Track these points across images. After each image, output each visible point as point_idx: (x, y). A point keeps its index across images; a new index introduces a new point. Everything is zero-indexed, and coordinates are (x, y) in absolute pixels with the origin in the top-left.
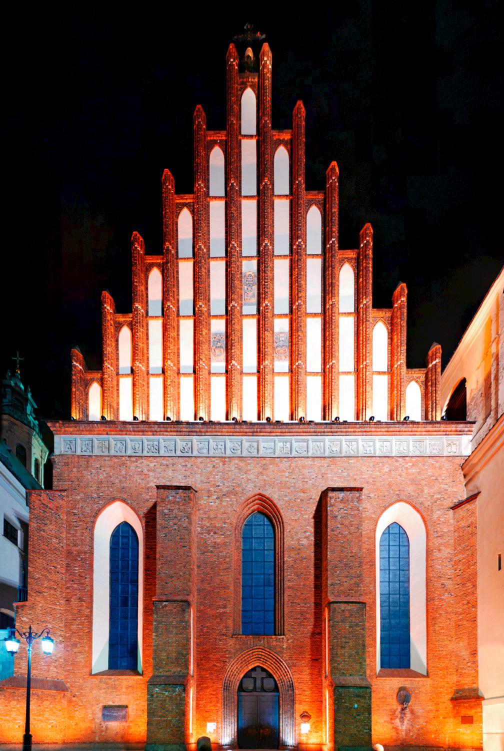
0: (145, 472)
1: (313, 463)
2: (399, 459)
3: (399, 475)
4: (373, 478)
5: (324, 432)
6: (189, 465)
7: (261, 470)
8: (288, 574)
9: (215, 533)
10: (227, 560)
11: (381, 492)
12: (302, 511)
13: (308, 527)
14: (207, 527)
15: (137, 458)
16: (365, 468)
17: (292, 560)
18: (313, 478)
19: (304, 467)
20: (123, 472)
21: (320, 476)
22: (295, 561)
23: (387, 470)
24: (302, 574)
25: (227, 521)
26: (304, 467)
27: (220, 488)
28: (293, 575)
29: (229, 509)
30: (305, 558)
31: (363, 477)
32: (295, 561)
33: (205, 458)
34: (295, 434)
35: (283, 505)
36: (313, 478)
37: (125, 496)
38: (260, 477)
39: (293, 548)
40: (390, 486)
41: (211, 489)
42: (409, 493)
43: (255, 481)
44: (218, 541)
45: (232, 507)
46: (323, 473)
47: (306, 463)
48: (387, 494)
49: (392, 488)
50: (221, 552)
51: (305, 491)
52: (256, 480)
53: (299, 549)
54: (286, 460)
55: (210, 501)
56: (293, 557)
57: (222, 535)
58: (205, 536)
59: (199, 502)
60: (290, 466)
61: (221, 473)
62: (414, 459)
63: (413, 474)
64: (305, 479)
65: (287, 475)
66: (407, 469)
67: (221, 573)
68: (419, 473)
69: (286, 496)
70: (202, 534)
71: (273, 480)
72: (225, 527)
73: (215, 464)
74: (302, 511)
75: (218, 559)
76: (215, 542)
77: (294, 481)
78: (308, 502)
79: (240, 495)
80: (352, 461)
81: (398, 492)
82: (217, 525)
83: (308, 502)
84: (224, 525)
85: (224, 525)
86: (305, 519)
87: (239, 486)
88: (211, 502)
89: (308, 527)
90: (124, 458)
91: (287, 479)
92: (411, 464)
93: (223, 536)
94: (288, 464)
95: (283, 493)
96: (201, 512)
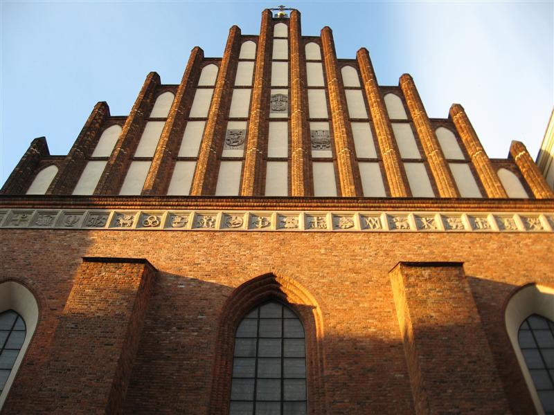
0: (75, 245)
1: (367, 239)
2: (509, 235)
3: (517, 252)
4: (474, 256)
5: (380, 207)
6: (151, 240)
7: (277, 245)
8: (337, 399)
9: (180, 328)
10: (199, 373)
11: (496, 272)
12: (356, 297)
13: (370, 321)
14: (166, 319)
15: (68, 231)
16: (457, 244)
17: (344, 374)
18: (371, 256)
19: (353, 243)
20: (37, 247)
21: (382, 254)
22: (350, 376)
23: (495, 246)
24: (368, 398)
25: (207, 310)
26: (353, 243)
27: (199, 266)
28: (346, 401)
29: (214, 294)
30: (372, 370)
31: (458, 254)
32: (350, 376)
33: (180, 232)
34: (333, 209)
35: (318, 288)
36: (371, 256)
37: (25, 274)
38: (275, 254)
39: (343, 353)
40: (507, 265)
41: (185, 267)
42: (545, 274)
43: (266, 259)
44: (186, 341)
45: (221, 291)
46: (386, 250)
47: (355, 239)
48: (508, 274)
49: (513, 267)
50: (189, 359)
51: (359, 271)
52: (268, 257)
53: (356, 355)
54: (319, 234)
55: (179, 283)
56: (345, 369)
57: (193, 331)
58: (159, 333)
59: (158, 284)
60: (327, 242)
61: (205, 249)
62: (532, 235)
63: (540, 251)
64: (356, 256)
65: (323, 251)
66: (526, 245)
67: (182, 397)
68: (549, 249)
69: (323, 277)
70: (153, 329)
71: (299, 257)
72: (201, 319)
73: (195, 238)
74: (356, 297)
75: (178, 371)
76: (178, 343)
77: (337, 259)
78: (365, 285)
79: (236, 276)
80: (432, 237)
81: (523, 272)
82: (187, 317)
83: (365, 285)
84: (200, 317)
85: (200, 317)
86: (364, 309)
87: (234, 263)
88: (181, 284)
89: (370, 321)
90: (45, 231)
91: (324, 257)
92: (530, 240)
93: (196, 334)
94: (322, 240)
95: (316, 273)
96: (159, 297)
